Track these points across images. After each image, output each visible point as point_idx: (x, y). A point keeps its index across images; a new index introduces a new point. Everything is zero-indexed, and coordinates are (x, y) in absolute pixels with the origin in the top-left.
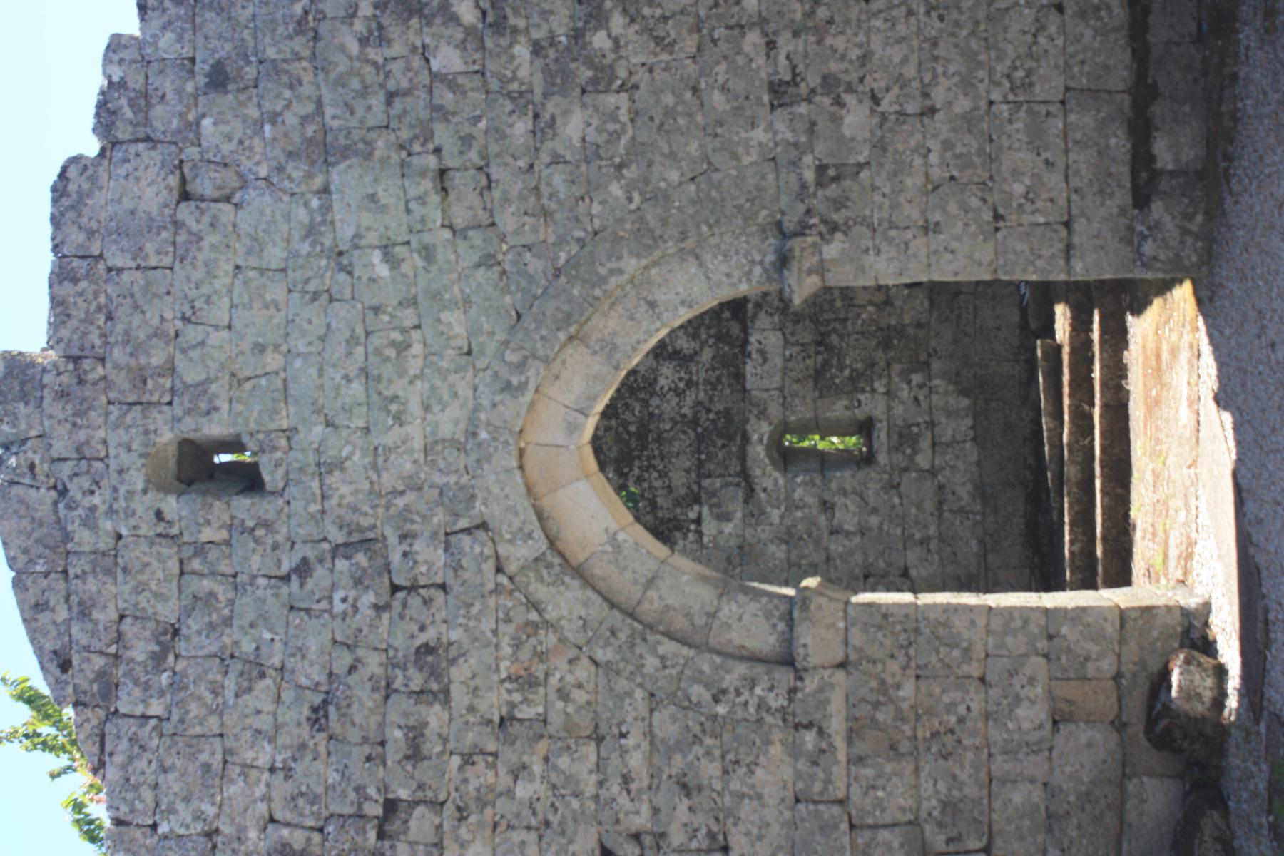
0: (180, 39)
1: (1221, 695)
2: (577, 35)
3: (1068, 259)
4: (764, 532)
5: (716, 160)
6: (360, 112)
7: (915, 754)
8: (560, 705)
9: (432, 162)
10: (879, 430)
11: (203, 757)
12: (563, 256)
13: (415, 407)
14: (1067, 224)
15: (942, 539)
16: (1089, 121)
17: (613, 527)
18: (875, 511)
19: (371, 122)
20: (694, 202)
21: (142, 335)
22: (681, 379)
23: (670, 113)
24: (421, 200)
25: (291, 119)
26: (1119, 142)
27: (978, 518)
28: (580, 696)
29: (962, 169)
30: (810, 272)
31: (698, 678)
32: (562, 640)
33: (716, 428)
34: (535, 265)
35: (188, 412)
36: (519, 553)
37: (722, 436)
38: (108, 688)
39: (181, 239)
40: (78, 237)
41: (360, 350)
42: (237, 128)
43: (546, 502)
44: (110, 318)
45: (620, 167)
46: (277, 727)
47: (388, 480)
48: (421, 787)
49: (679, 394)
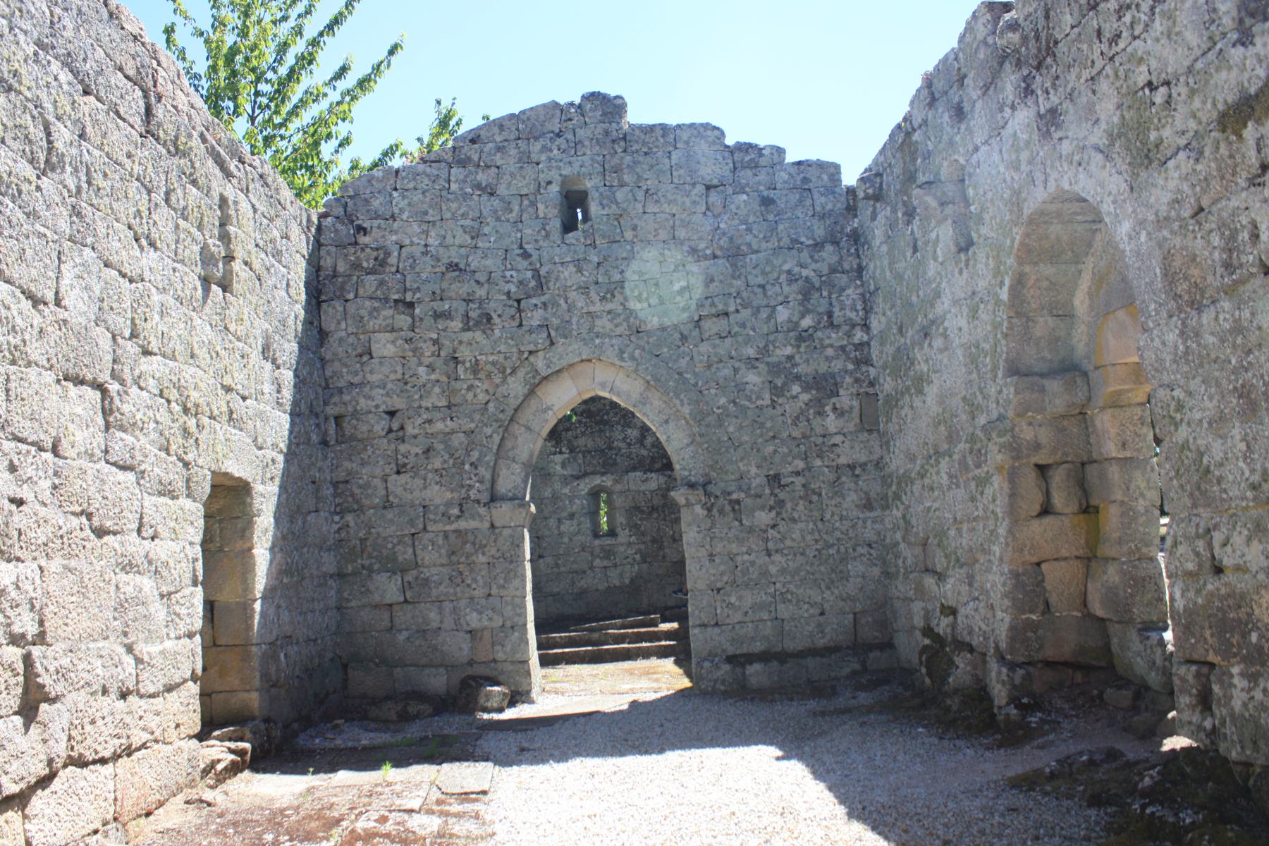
0: (785, 182)
1: (489, 711)
2: (798, 377)
3: (700, 626)
4: (557, 486)
5: (740, 450)
6: (754, 272)
7: (451, 564)
8: (465, 386)
9: (732, 309)
11: (431, 211)
12: (688, 376)
13: (609, 306)
14: (717, 624)
15: (558, 574)
16: (768, 631)
17: (555, 408)
18: (571, 540)
19: (750, 278)
20: (719, 440)
21: (638, 170)
23: (762, 425)
24: (713, 304)
25: (749, 238)
26: (758, 647)
28: (470, 396)
29: (742, 572)
30: (687, 499)
31: (482, 455)
32: (497, 386)
34: (683, 362)
35: (601, 194)
36: (539, 362)
38: (463, 163)
39: (687, 187)
40: (685, 136)
41: (636, 277)
42: (743, 212)
43: (565, 374)
44: (646, 154)
45: (734, 402)
46: (447, 247)
47: (573, 295)
48: (421, 319)
49: (624, 440)
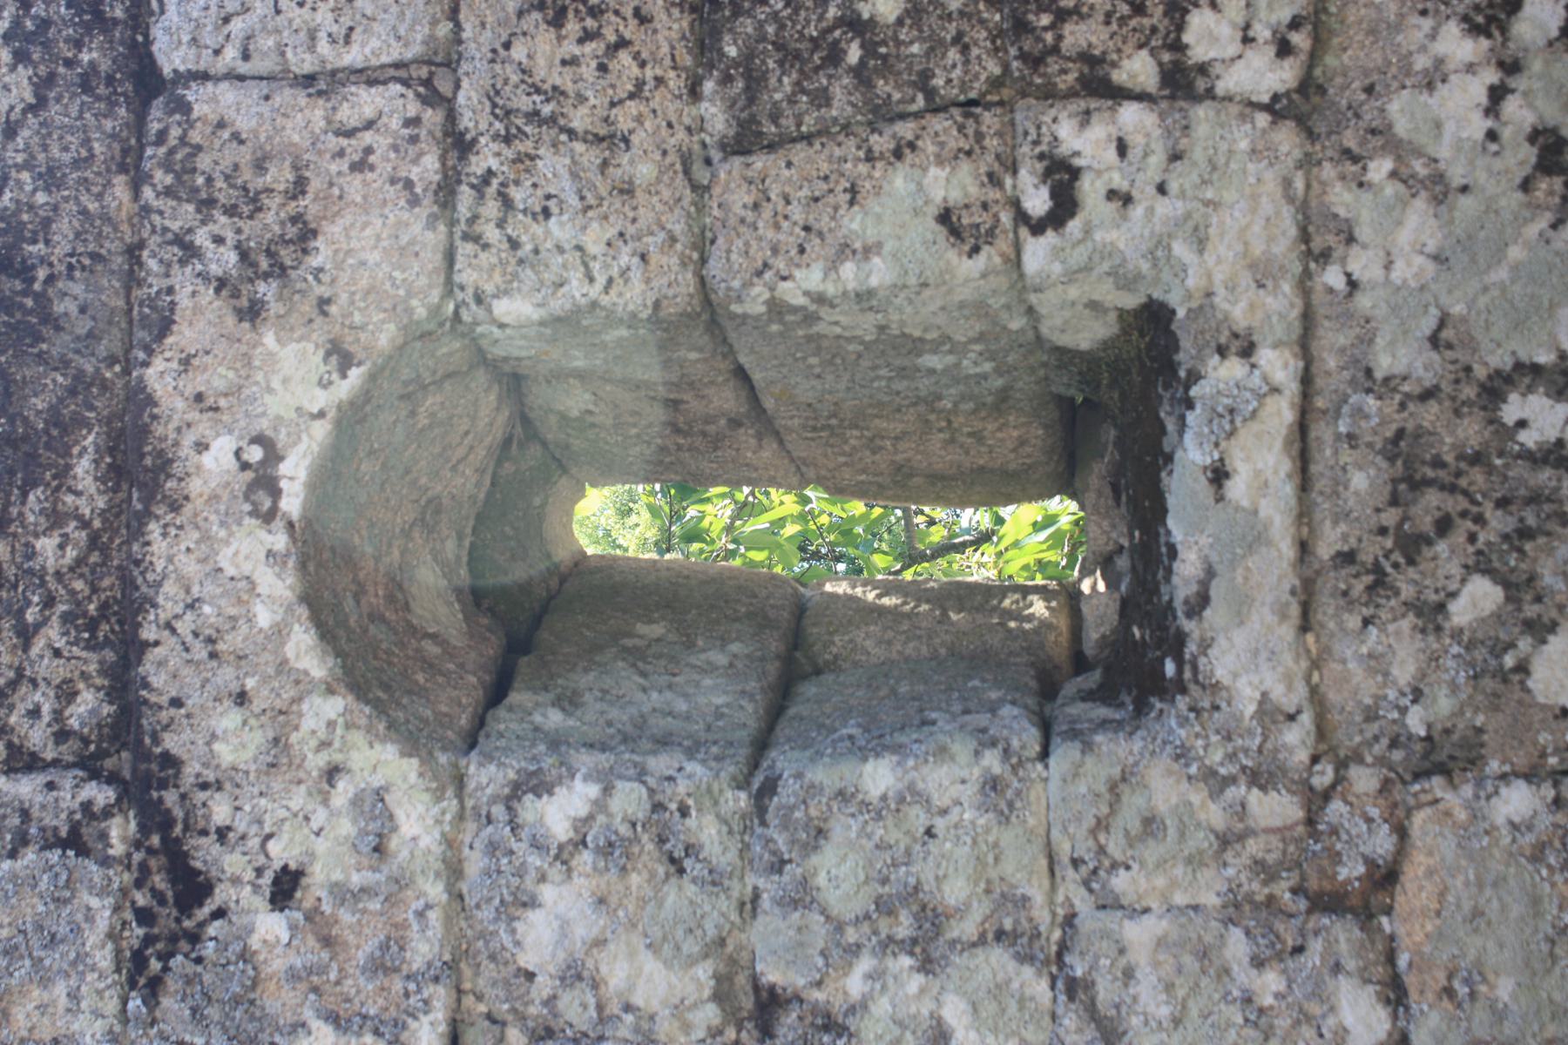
10: (1230, 418)
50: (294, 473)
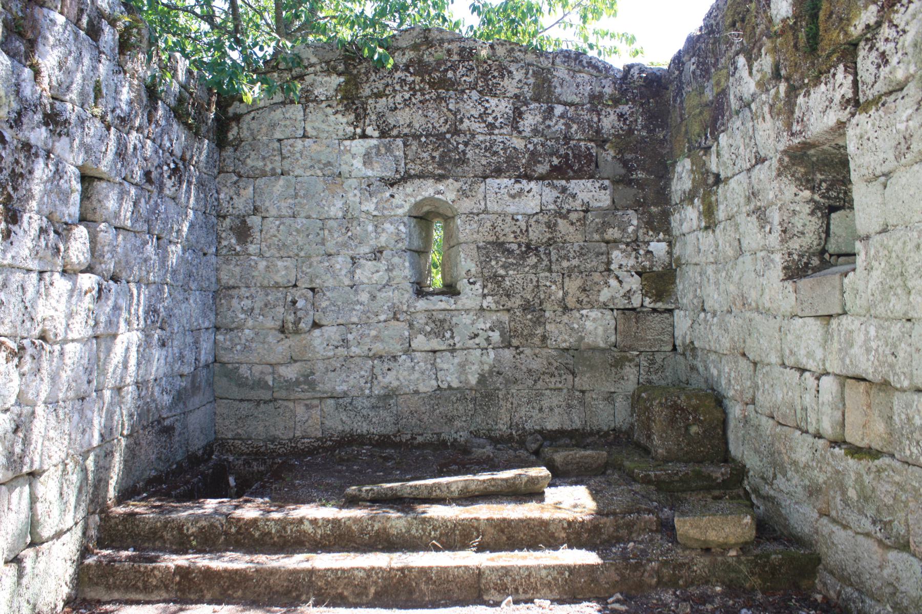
4: (353, 197)
10: (447, 302)
15: (347, 358)
18: (373, 298)
22: (496, 118)
27: (367, 392)
33: (449, 151)
37: (442, 156)
49: (482, 117)
50: (440, 196)
